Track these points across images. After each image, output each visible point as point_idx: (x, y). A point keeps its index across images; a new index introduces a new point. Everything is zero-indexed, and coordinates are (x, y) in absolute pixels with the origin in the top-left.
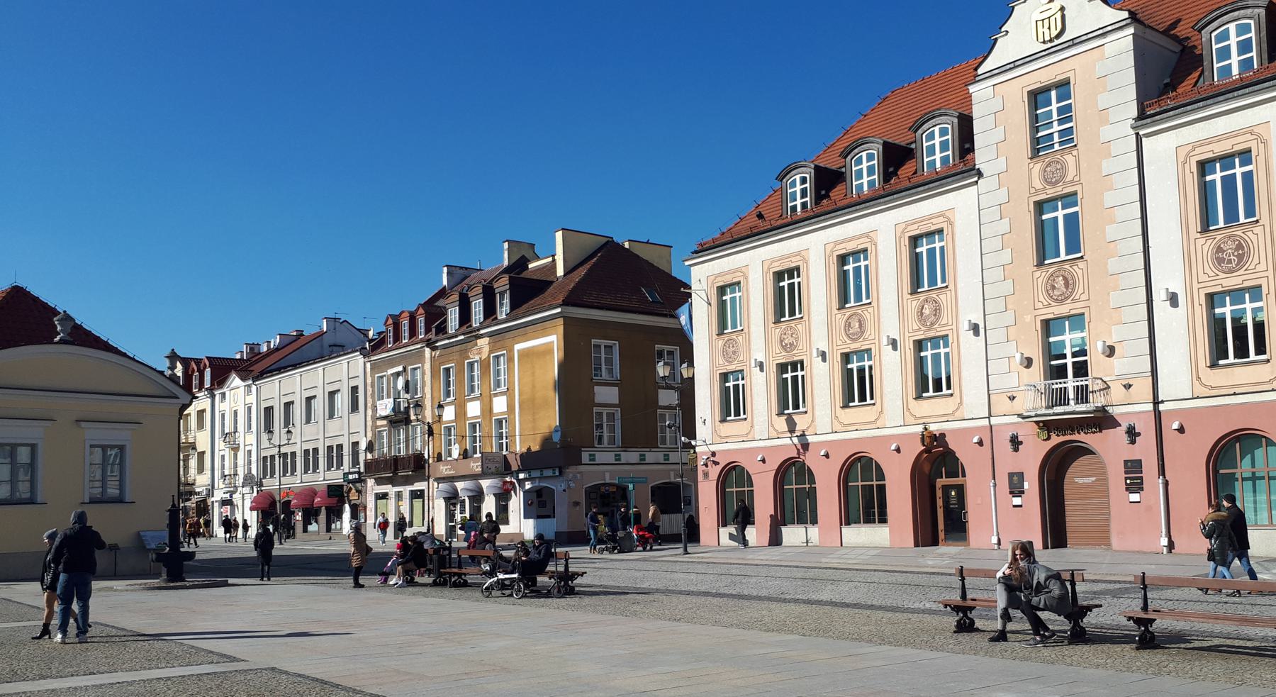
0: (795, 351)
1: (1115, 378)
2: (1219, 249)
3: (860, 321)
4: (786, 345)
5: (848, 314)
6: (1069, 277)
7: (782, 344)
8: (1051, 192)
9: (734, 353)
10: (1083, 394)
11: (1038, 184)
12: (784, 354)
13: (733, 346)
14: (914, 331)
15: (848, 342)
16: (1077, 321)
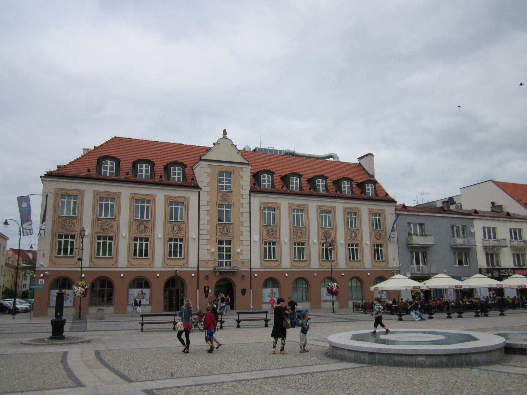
0: (109, 232)
1: (240, 260)
2: (268, 231)
3: (145, 226)
4: (104, 228)
5: (139, 222)
6: (228, 228)
7: (101, 228)
8: (224, 202)
9: (70, 226)
10: (228, 264)
11: (220, 199)
12: (102, 232)
13: (69, 223)
14: (169, 234)
15: (138, 233)
16: (229, 242)
